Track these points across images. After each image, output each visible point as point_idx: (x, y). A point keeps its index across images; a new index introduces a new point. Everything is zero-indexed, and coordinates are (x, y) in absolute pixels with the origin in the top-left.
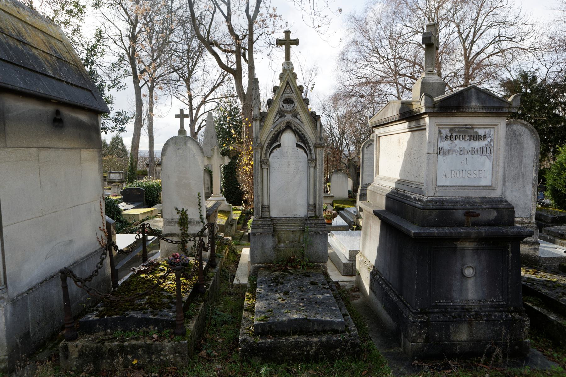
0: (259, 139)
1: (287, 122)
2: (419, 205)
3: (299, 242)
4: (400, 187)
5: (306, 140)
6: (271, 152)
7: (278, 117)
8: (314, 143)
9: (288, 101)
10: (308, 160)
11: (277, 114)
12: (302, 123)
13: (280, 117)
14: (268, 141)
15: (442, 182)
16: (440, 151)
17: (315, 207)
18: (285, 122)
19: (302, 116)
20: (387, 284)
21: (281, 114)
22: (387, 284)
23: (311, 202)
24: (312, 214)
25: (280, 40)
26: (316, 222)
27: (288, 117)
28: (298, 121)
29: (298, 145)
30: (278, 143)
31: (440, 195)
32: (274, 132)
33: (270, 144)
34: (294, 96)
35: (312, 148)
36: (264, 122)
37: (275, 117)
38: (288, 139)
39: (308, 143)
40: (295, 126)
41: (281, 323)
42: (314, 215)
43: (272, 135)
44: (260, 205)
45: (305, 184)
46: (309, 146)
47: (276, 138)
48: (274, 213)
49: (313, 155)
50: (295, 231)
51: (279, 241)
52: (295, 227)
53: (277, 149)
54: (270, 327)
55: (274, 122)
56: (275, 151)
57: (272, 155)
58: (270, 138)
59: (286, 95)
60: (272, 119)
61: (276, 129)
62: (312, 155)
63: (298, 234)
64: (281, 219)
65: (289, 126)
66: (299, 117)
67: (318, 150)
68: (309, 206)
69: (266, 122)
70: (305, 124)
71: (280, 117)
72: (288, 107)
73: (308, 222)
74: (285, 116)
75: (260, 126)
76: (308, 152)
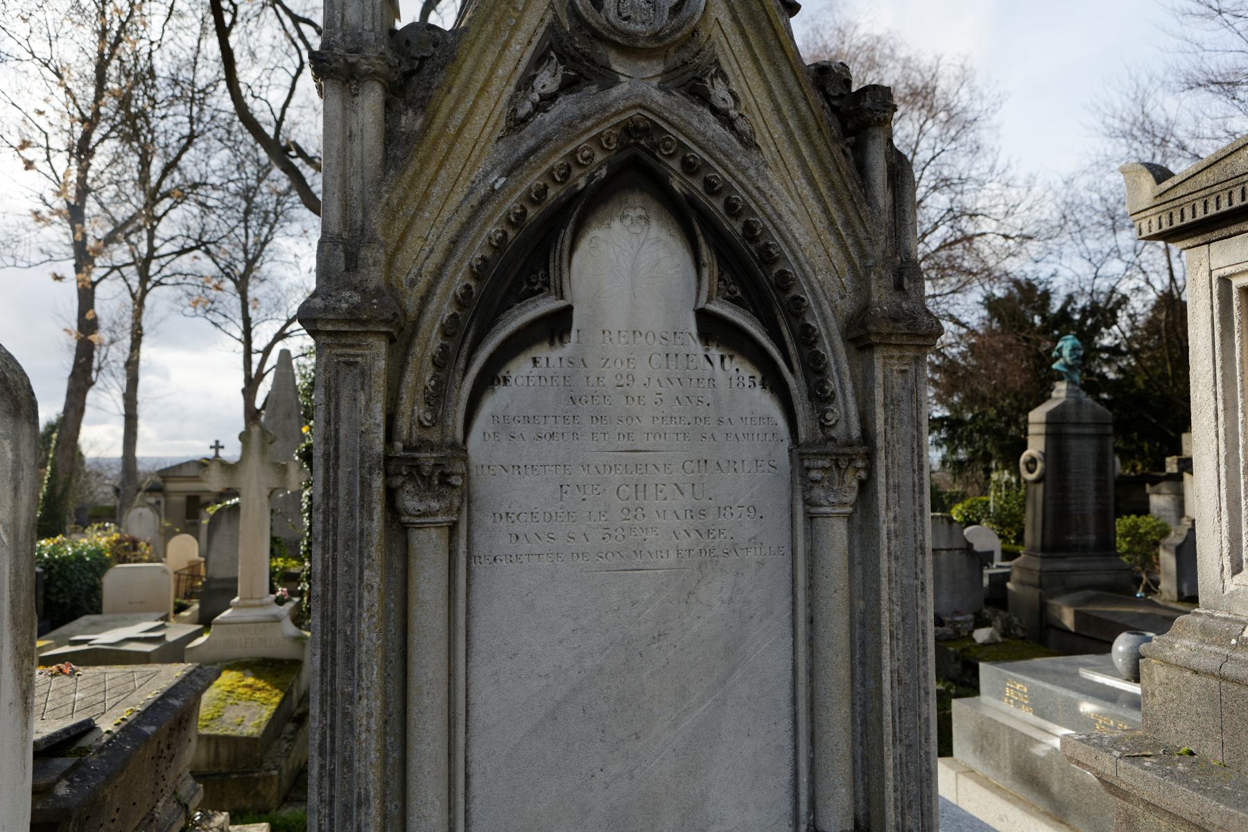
0: (372, 255)
1: (630, 130)
5: (784, 282)
6: (489, 378)
7: (547, 81)
8: (847, 306)
10: (799, 451)
11: (539, 60)
12: (749, 143)
13: (568, 86)
14: (458, 279)
19: (744, 82)
27: (637, 85)
28: (715, 128)
29: (711, 328)
30: (546, 305)
32: (512, 204)
35: (833, 348)
36: (422, 106)
37: (526, 83)
38: (630, 271)
39: (796, 308)
40: (690, 168)
45: (770, 652)
46: (807, 337)
49: (844, 414)
55: (517, 124)
56: (520, 368)
57: (493, 403)
58: (476, 250)
60: (502, 89)
61: (533, 179)
65: (639, 169)
66: (719, 92)
70: (768, 153)
71: (568, 86)
74: (609, 79)
76: (795, 384)
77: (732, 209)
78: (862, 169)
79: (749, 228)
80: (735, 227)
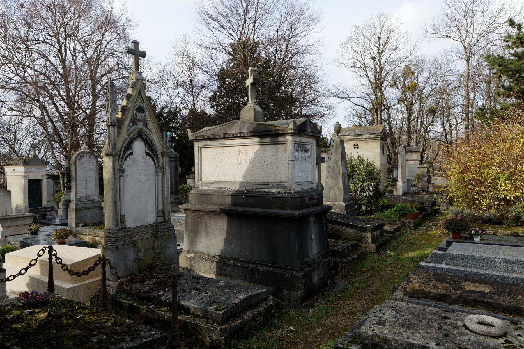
2: (288, 195)
3: (153, 248)
4: (243, 186)
5: (155, 148)
6: (125, 160)
7: (131, 125)
9: (140, 110)
10: (156, 168)
11: (130, 122)
12: (151, 132)
13: (133, 125)
14: (123, 149)
15: (297, 180)
16: (296, 159)
17: (164, 213)
18: (137, 131)
20: (249, 263)
21: (134, 121)
22: (249, 263)
23: (160, 208)
24: (160, 219)
25: (131, 49)
26: (166, 226)
27: (140, 125)
28: (148, 130)
29: (147, 154)
30: (131, 151)
31: (301, 188)
32: (128, 140)
33: (125, 152)
34: (144, 106)
35: (160, 156)
37: (129, 125)
38: (139, 146)
39: (156, 151)
40: (145, 135)
41: (237, 305)
42: (163, 220)
43: (126, 143)
44: (119, 215)
45: (153, 191)
46: (157, 155)
47: (129, 146)
48: (129, 223)
49: (161, 164)
50: (149, 238)
51: (138, 251)
52: (149, 234)
53: (130, 156)
54: (231, 312)
55: (128, 130)
56: (128, 158)
57: (126, 162)
58: (125, 146)
59: (139, 104)
61: (130, 137)
62: (160, 163)
63: (152, 241)
64: (135, 228)
65: (140, 135)
66: (148, 126)
67: (165, 158)
68: (158, 211)
69: (123, 129)
71: (133, 125)
72: (140, 116)
73: (161, 227)
74: (137, 125)
75: (117, 132)
76: (155, 160)
77: (149, 140)
78: (163, 135)
79: (151, 142)
80: (150, 142)
